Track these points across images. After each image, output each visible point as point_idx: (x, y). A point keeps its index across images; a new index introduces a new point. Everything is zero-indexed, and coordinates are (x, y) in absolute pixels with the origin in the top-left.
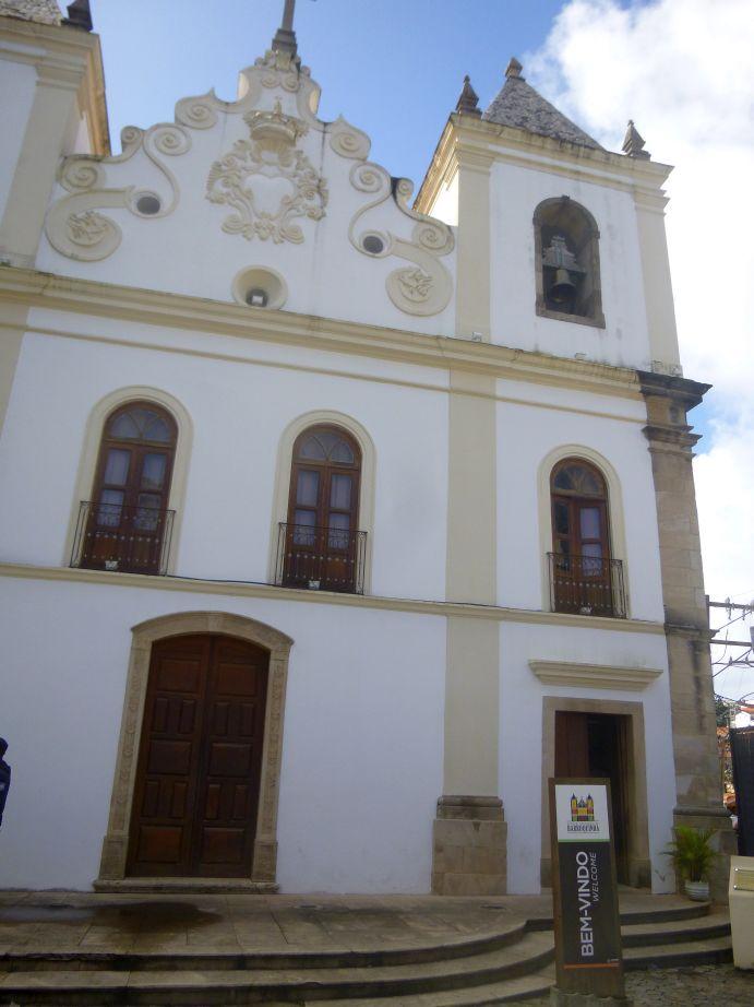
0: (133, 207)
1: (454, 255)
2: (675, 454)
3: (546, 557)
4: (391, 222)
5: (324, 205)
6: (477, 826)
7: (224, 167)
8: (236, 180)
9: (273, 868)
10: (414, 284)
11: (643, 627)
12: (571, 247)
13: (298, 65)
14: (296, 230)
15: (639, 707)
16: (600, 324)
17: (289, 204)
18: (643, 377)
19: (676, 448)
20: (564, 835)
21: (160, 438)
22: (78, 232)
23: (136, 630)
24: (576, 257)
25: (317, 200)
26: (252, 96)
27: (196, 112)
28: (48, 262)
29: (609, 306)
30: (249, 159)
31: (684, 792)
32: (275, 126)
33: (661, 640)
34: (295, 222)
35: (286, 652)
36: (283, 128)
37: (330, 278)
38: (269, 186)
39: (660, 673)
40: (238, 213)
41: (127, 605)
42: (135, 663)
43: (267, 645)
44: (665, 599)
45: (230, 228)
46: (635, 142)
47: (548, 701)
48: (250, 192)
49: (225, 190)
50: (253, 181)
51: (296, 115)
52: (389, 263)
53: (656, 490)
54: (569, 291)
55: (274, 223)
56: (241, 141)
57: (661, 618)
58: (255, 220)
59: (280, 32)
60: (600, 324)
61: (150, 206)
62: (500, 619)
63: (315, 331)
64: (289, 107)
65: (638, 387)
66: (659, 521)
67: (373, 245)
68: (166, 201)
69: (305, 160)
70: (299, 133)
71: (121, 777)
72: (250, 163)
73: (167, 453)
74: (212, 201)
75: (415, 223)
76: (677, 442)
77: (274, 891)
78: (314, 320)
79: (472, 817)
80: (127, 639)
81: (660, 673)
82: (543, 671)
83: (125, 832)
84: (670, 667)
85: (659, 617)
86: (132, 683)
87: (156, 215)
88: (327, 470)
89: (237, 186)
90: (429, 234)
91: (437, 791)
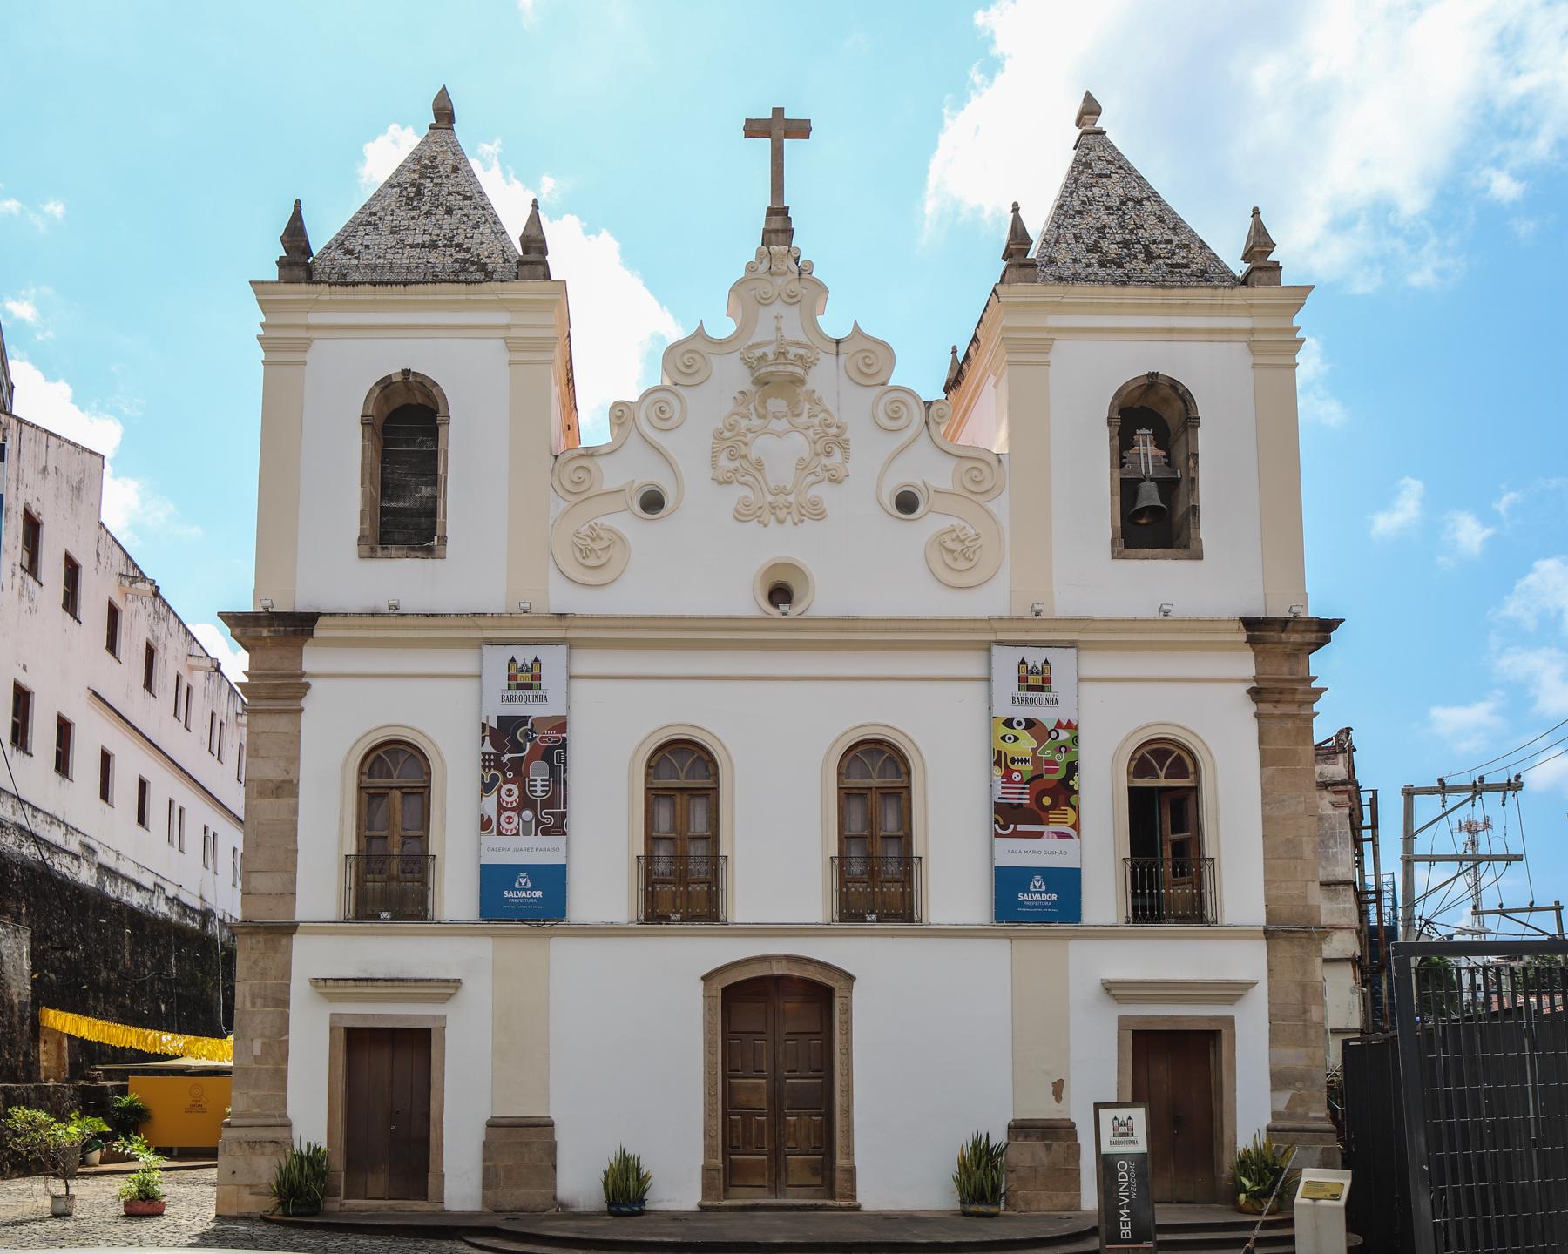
0: (637, 507)
1: (1004, 499)
2: (1289, 716)
3: (1121, 864)
4: (927, 471)
5: (847, 459)
6: (1048, 1147)
7: (727, 434)
8: (744, 450)
9: (854, 1189)
10: (957, 547)
11: (1238, 933)
12: (1164, 439)
13: (797, 260)
14: (815, 503)
15: (1230, 1021)
16: (1199, 556)
17: (802, 465)
19: (1291, 709)
20: (1106, 1148)
22: (586, 552)
23: (706, 978)
24: (1168, 456)
25: (838, 455)
26: (746, 326)
27: (687, 359)
28: (562, 597)
29: (1207, 529)
30: (754, 417)
31: (1281, 1107)
32: (781, 368)
33: (1261, 945)
34: (815, 491)
35: (850, 990)
36: (791, 368)
37: (865, 567)
38: (782, 448)
39: (1252, 984)
40: (747, 492)
41: (691, 957)
42: (708, 1010)
43: (830, 983)
44: (1267, 899)
45: (740, 517)
46: (1259, 245)
47: (1123, 1021)
48: (759, 462)
50: (761, 446)
51: (804, 340)
52: (928, 524)
53: (1264, 763)
54: (1155, 518)
55: (791, 498)
56: (742, 393)
57: (1261, 919)
58: (770, 498)
59: (771, 212)
60: (1199, 556)
61: (653, 502)
62: (1070, 938)
64: (793, 331)
66: (1264, 804)
67: (907, 503)
69: (818, 402)
71: (709, 1114)
73: (710, 795)
74: (720, 483)
75: (953, 462)
76: (1293, 701)
77: (857, 1208)
79: (1043, 1139)
81: (1252, 984)
83: (719, 1162)
84: (1270, 976)
85: (1259, 918)
86: (708, 1029)
87: (663, 513)
89: (744, 457)
90: (975, 473)
91: (1008, 1117)
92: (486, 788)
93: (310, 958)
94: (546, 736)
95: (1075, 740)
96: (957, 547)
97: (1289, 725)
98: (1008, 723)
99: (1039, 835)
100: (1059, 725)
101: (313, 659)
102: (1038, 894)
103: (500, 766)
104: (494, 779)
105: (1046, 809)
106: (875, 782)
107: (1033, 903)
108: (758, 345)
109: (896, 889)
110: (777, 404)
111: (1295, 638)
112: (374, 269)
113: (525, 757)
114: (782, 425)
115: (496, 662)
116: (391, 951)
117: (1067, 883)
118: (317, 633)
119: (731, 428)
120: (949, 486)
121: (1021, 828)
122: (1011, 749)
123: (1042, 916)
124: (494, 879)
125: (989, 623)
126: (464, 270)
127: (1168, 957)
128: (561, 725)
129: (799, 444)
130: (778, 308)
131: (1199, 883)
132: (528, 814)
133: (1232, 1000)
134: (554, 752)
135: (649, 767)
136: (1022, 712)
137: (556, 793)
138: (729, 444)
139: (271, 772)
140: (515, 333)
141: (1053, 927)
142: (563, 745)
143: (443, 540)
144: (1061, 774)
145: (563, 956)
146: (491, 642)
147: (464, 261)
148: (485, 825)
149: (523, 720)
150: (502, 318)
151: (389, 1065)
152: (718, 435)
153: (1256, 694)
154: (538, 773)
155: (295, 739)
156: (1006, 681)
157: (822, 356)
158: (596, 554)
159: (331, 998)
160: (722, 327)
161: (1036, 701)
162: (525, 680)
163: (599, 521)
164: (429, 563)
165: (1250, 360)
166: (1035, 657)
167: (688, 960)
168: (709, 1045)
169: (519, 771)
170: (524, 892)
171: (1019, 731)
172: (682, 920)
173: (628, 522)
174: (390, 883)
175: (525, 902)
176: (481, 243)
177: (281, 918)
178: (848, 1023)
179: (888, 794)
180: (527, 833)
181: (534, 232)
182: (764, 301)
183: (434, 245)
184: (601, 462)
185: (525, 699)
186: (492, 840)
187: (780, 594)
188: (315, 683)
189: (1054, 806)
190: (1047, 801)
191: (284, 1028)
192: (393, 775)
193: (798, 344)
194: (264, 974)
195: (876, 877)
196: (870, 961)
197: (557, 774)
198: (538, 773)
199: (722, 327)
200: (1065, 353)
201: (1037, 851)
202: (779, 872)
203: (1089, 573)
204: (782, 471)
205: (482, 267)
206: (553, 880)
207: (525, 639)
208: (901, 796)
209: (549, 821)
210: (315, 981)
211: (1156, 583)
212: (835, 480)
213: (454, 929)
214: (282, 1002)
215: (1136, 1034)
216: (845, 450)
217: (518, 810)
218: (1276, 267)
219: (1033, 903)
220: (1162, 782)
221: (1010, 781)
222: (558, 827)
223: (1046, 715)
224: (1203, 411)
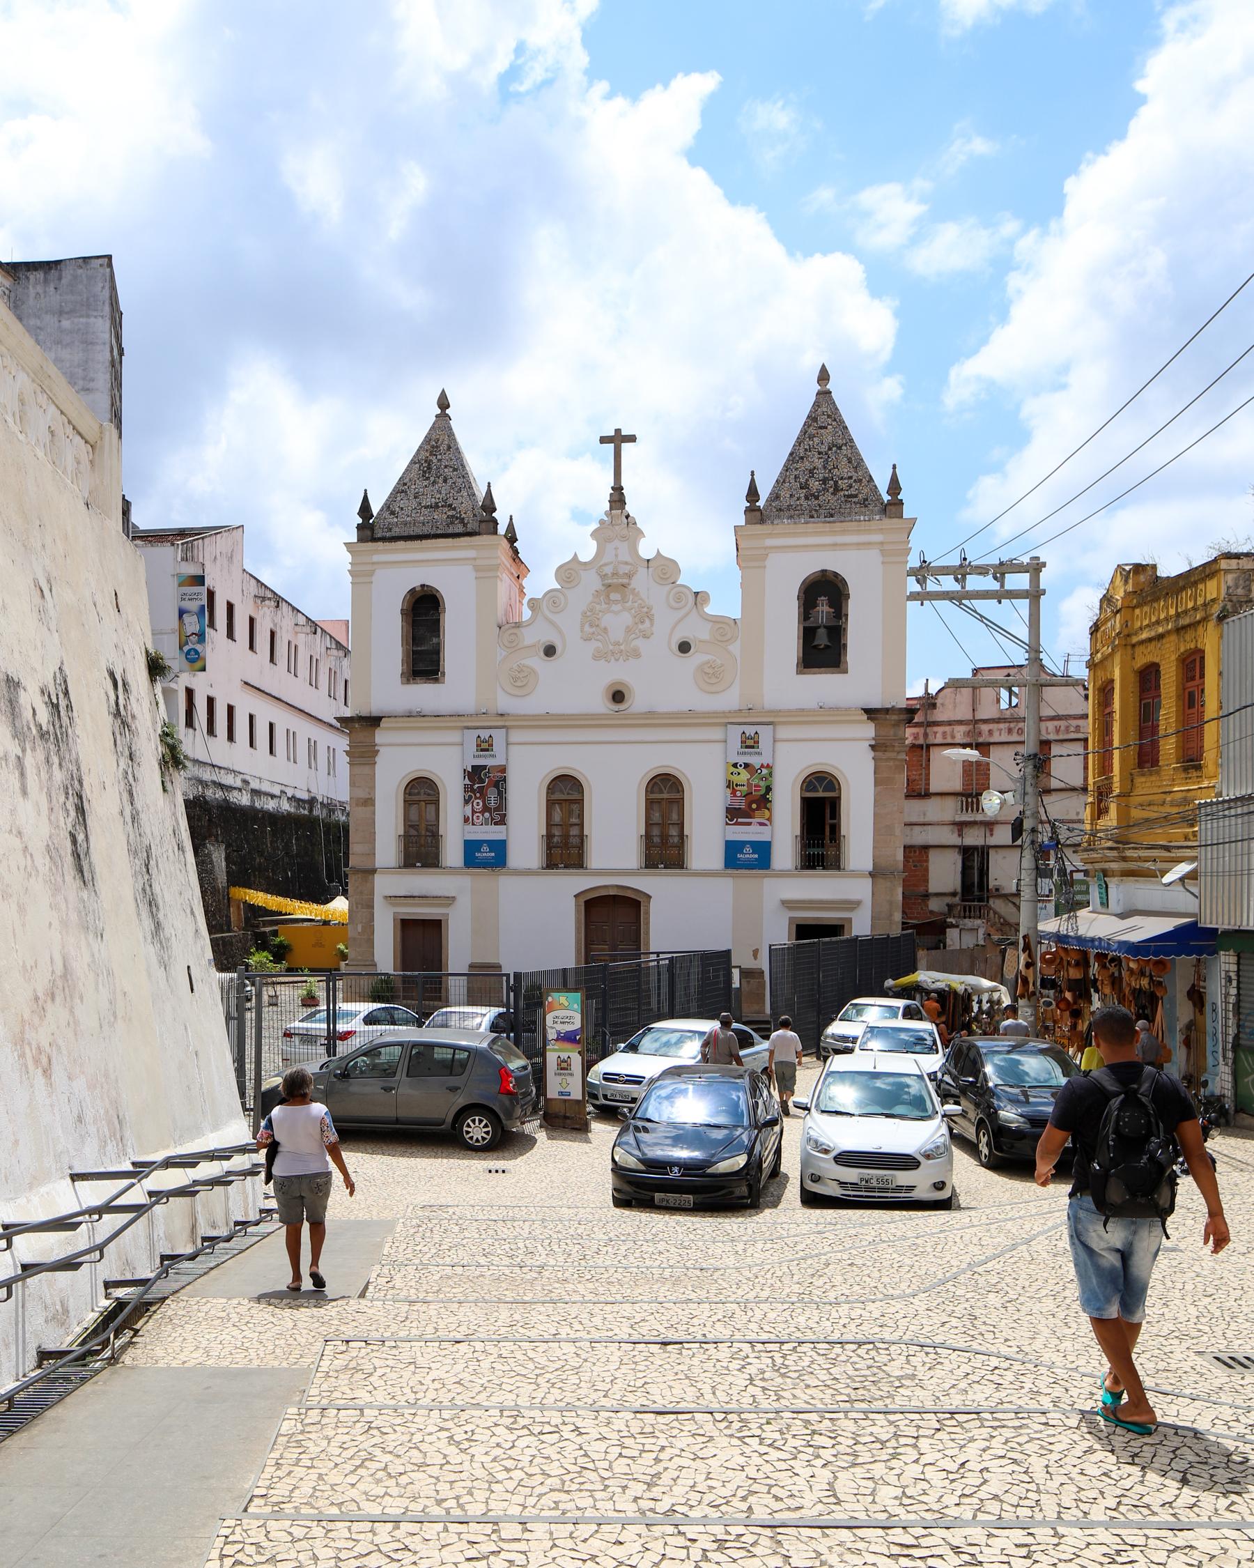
0: (542, 654)
5: (652, 625)
10: (711, 671)
11: (856, 874)
17: (628, 630)
18: (868, 711)
19: (893, 755)
21: (576, 796)
22: (515, 679)
25: (647, 622)
28: (505, 703)
29: (853, 654)
33: (868, 882)
34: (635, 643)
40: (600, 644)
42: (577, 911)
45: (597, 656)
46: (895, 486)
48: (605, 629)
49: (591, 630)
50: (607, 620)
51: (629, 559)
52: (695, 658)
63: (652, 719)
64: (624, 556)
65: (865, 717)
67: (684, 647)
70: (629, 576)
72: (604, 606)
78: (651, 714)
80: (572, 903)
82: (788, 904)
85: (870, 868)
86: (578, 921)
92: (466, 802)
93: (384, 885)
94: (495, 775)
95: (770, 774)
96: (711, 671)
97: (891, 763)
98: (735, 765)
99: (750, 824)
100: (762, 766)
101: (381, 736)
102: (748, 855)
103: (473, 790)
104: (470, 797)
105: (754, 810)
106: (665, 796)
107: (746, 859)
108: (605, 565)
109: (675, 851)
110: (614, 596)
111: (895, 717)
112: (405, 524)
113: (486, 786)
114: (616, 608)
115: (471, 737)
116: (421, 882)
117: (763, 851)
118: (383, 723)
119: (591, 610)
122: (735, 779)
123: (749, 866)
124: (471, 848)
125: (724, 714)
126: (452, 523)
127: (819, 888)
128: (503, 769)
129: (627, 618)
130: (616, 543)
131: (838, 848)
132: (487, 815)
133: (852, 909)
134: (500, 784)
135: (548, 788)
136: (742, 760)
137: (501, 803)
138: (590, 620)
139: (362, 794)
140: (479, 562)
141: (754, 872)
142: (505, 780)
143: (443, 674)
144: (763, 792)
145: (505, 884)
146: (468, 728)
148: (466, 820)
149: (484, 767)
150: (471, 553)
152: (584, 614)
154: (492, 795)
155: (373, 777)
156: (735, 742)
157: (640, 569)
158: (522, 680)
159: (394, 905)
160: (588, 551)
161: (750, 754)
162: (485, 746)
163: (523, 662)
164: (436, 685)
165: (881, 559)
166: (750, 730)
167: (567, 888)
168: (578, 929)
169: (482, 793)
170: (486, 853)
171: (741, 769)
172: (565, 867)
173: (537, 662)
174: (421, 849)
175: (486, 858)
176: (463, 504)
177: (369, 866)
178: (648, 919)
179: (671, 802)
180: (487, 824)
181: (488, 503)
182: (609, 540)
184: (523, 630)
185: (485, 756)
186: (470, 827)
187: (618, 696)
188: (382, 750)
189: (758, 809)
190: (754, 806)
191: (372, 919)
192: (421, 792)
193: (626, 563)
194: (361, 893)
196: (660, 889)
197: (502, 795)
198: (492, 795)
199: (588, 551)
200: (774, 560)
201: (749, 832)
202: (614, 844)
203: (782, 680)
204: (617, 634)
206: (500, 848)
207: (486, 727)
208: (678, 803)
209: (498, 818)
210: (386, 897)
211: (823, 685)
212: (645, 637)
213: (453, 870)
214: (371, 906)
215: (798, 927)
216: (651, 620)
217: (482, 812)
218: (901, 503)
219: (746, 859)
220: (821, 794)
222: (502, 821)
223: (755, 761)
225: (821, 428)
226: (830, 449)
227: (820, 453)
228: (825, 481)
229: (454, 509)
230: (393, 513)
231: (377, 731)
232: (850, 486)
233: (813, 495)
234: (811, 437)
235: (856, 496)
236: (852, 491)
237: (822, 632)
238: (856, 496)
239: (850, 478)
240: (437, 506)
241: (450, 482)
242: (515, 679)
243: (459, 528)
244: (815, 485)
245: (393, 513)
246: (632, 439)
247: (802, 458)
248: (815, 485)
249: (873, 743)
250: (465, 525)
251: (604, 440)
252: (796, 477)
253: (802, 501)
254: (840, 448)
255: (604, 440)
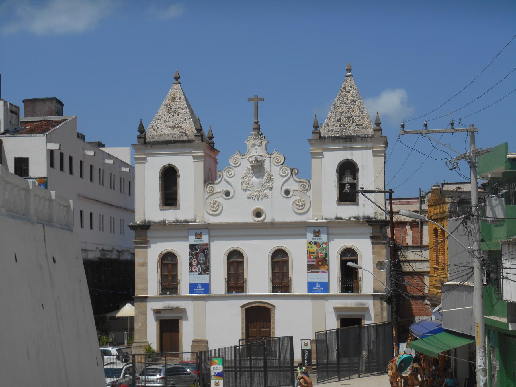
0: (224, 196)
1: (311, 191)
16: (358, 204)
40: (249, 192)
45: (249, 198)
60: (358, 204)
63: (273, 225)
67: (287, 192)
68: (232, 195)
88: (280, 260)
99: (318, 272)
101: (150, 233)
112: (160, 135)
118: (151, 228)
120: (298, 189)
121: (313, 270)
126: (182, 135)
143: (179, 205)
147: (182, 132)
151: (169, 327)
153: (372, 238)
163: (217, 200)
174: (169, 284)
183: (175, 127)
189: (322, 265)
190: (320, 263)
193: (261, 156)
195: (280, 282)
202: (258, 280)
205: (186, 134)
221: (310, 258)
224: (360, 168)
225: (347, 92)
226: (351, 103)
227: (346, 104)
228: (348, 118)
229: (183, 129)
230: (154, 130)
231: (148, 231)
232: (359, 120)
233: (343, 124)
234: (343, 97)
235: (362, 125)
236: (360, 123)
237: (347, 186)
238: (362, 125)
239: (359, 116)
240: (175, 127)
241: (181, 115)
242: (213, 207)
243: (185, 138)
244: (344, 120)
245: (154, 130)
246: (263, 100)
247: (338, 107)
248: (344, 120)
249: (371, 236)
250: (188, 136)
251: (250, 100)
252: (336, 116)
253: (338, 127)
254: (355, 102)
255: (250, 100)
